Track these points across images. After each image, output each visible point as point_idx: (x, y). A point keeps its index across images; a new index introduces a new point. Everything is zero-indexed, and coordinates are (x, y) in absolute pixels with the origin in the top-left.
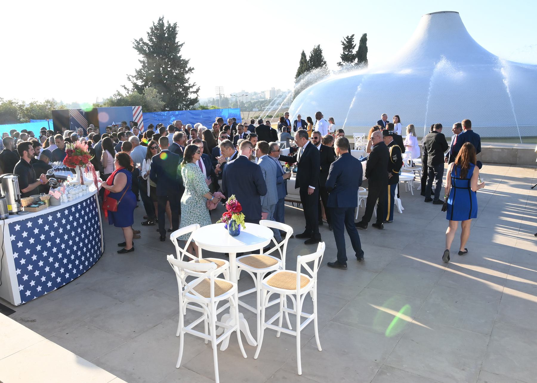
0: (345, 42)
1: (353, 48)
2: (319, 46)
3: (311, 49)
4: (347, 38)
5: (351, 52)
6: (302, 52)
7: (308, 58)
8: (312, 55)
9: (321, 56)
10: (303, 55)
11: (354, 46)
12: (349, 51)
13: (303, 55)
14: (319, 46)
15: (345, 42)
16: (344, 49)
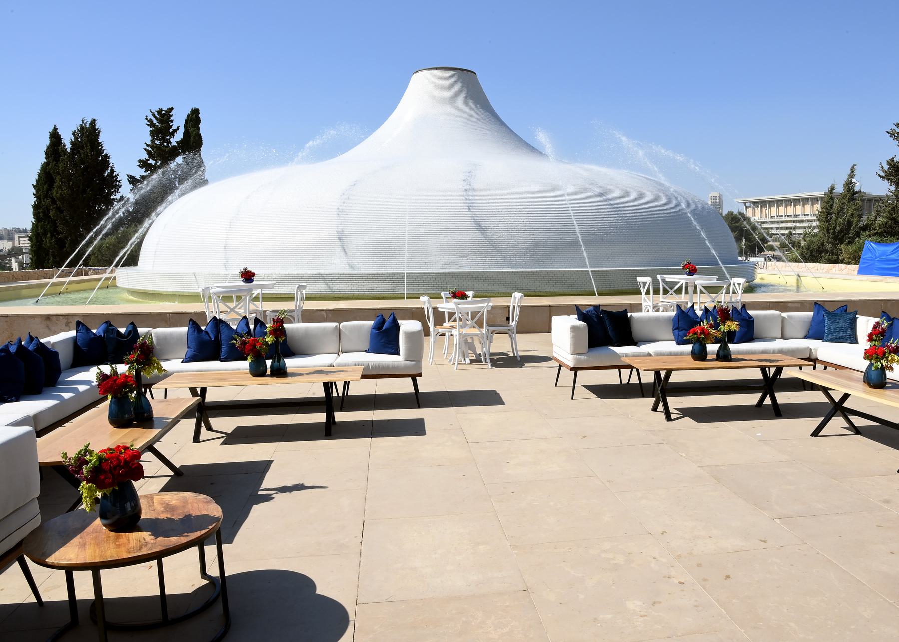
0: (155, 121)
1: (172, 135)
2: (93, 122)
3: (75, 126)
4: (160, 111)
8: (76, 139)
9: (100, 144)
10: (55, 136)
11: (176, 131)
12: (164, 140)
13: (55, 136)
14: (93, 122)
15: (155, 121)
16: (153, 134)
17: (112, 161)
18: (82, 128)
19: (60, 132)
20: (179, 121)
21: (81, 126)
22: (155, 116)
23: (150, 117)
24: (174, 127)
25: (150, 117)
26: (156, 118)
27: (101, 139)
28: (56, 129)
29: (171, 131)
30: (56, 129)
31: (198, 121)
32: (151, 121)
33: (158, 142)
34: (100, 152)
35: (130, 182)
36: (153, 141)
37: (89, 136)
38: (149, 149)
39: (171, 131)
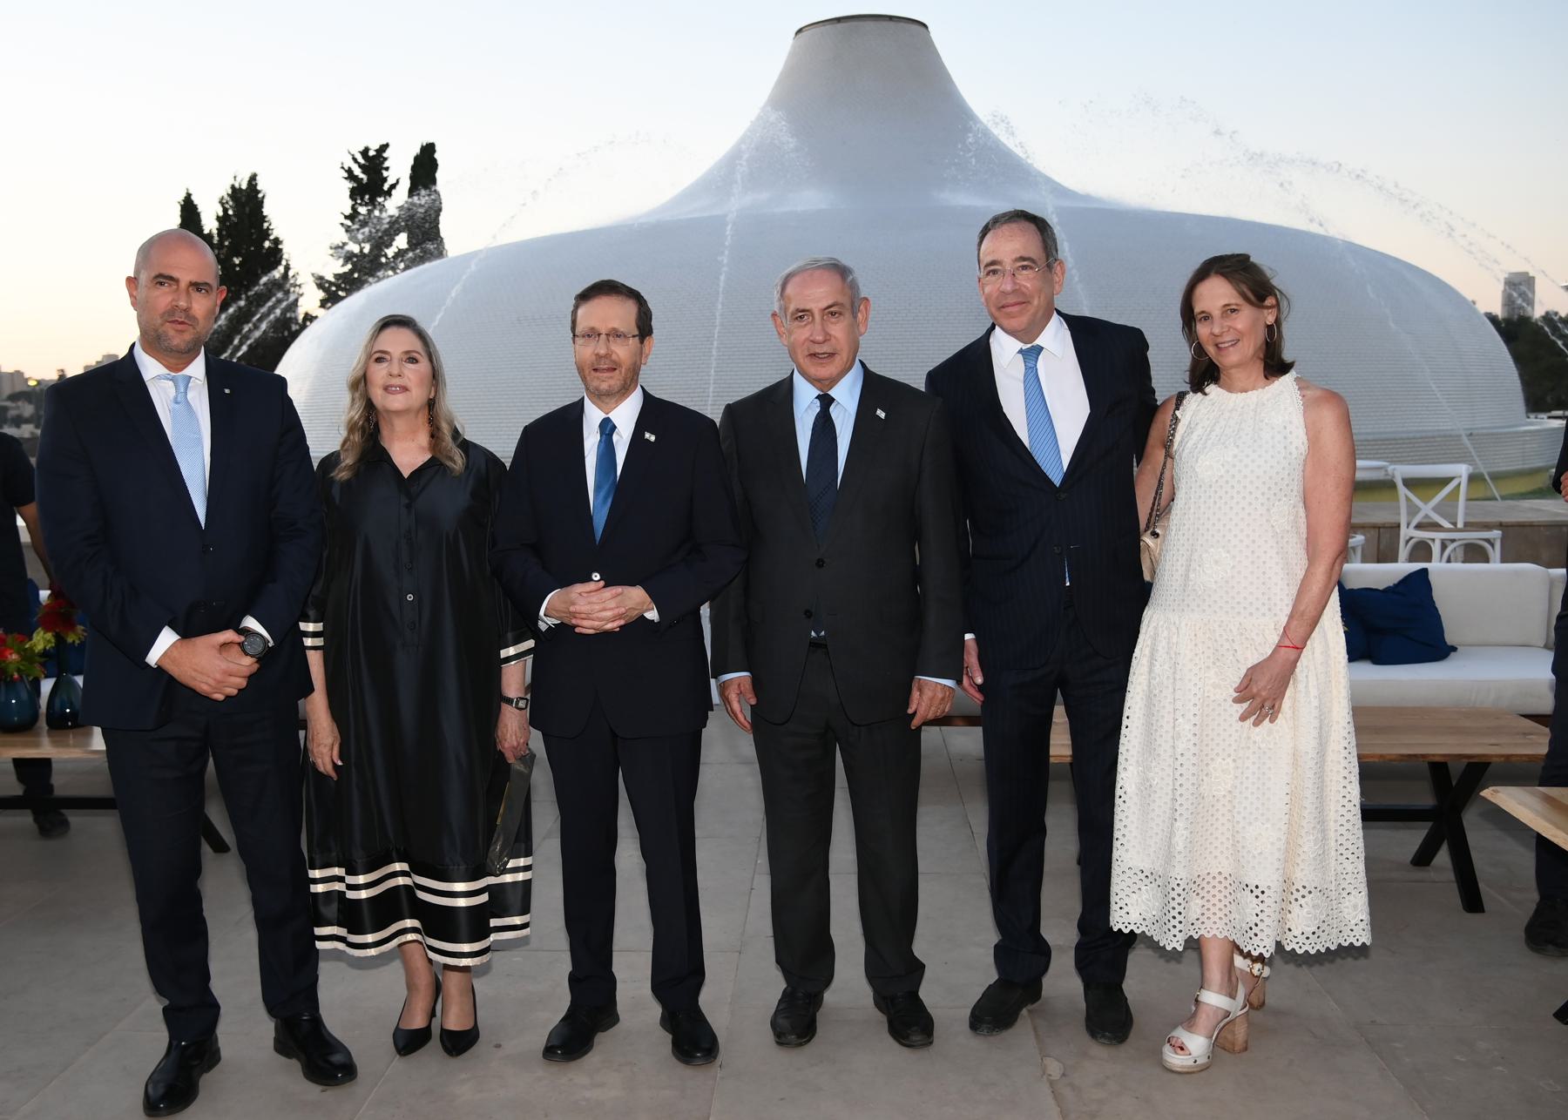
0: (357, 171)
1: (389, 193)
2: (253, 178)
3: (225, 191)
4: (365, 153)
5: (383, 208)
6: (182, 196)
7: (210, 224)
8: (225, 210)
9: (263, 219)
11: (393, 187)
14: (253, 178)
15: (357, 171)
16: (354, 194)
17: (286, 248)
18: (235, 192)
19: (196, 199)
20: (399, 169)
21: (233, 187)
22: (355, 160)
23: (350, 163)
24: (391, 181)
25: (350, 163)
26: (360, 166)
27: (266, 211)
28: (189, 196)
29: (386, 187)
30: (189, 196)
31: (434, 165)
32: (350, 171)
33: (363, 210)
34: (265, 234)
35: (320, 286)
36: (353, 208)
37: (246, 205)
38: (348, 223)
39: (386, 187)
